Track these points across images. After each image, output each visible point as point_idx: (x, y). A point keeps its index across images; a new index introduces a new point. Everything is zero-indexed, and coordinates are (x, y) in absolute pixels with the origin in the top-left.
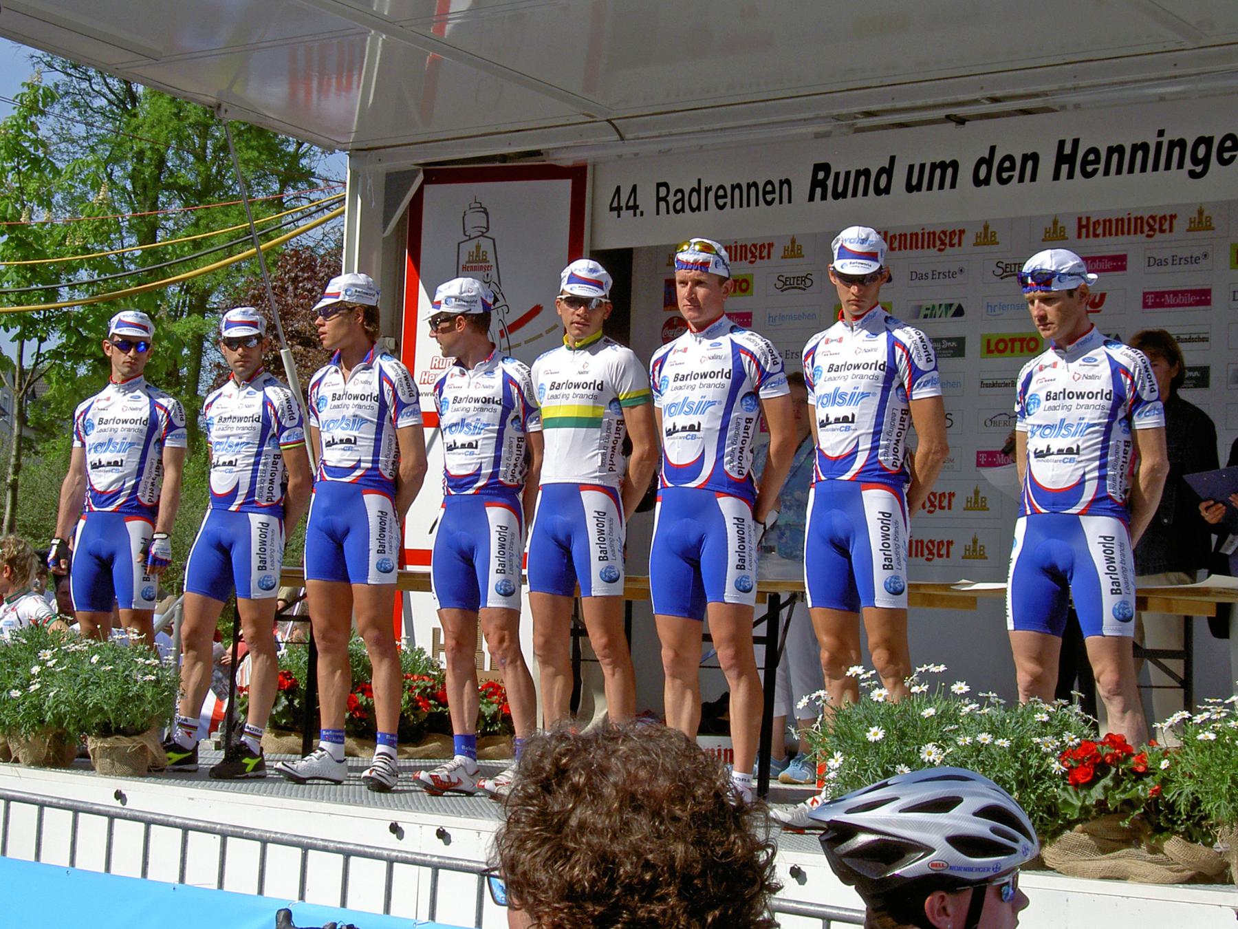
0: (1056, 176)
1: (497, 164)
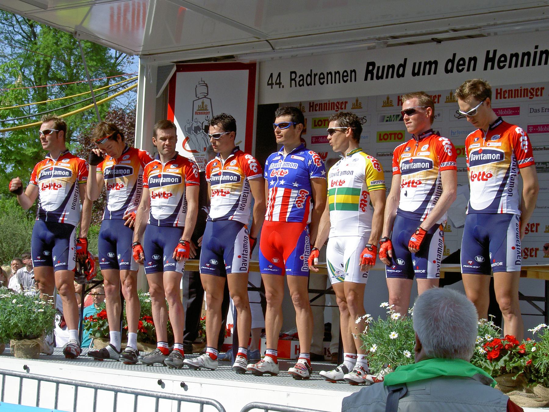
0: (485, 68)
1: (213, 62)
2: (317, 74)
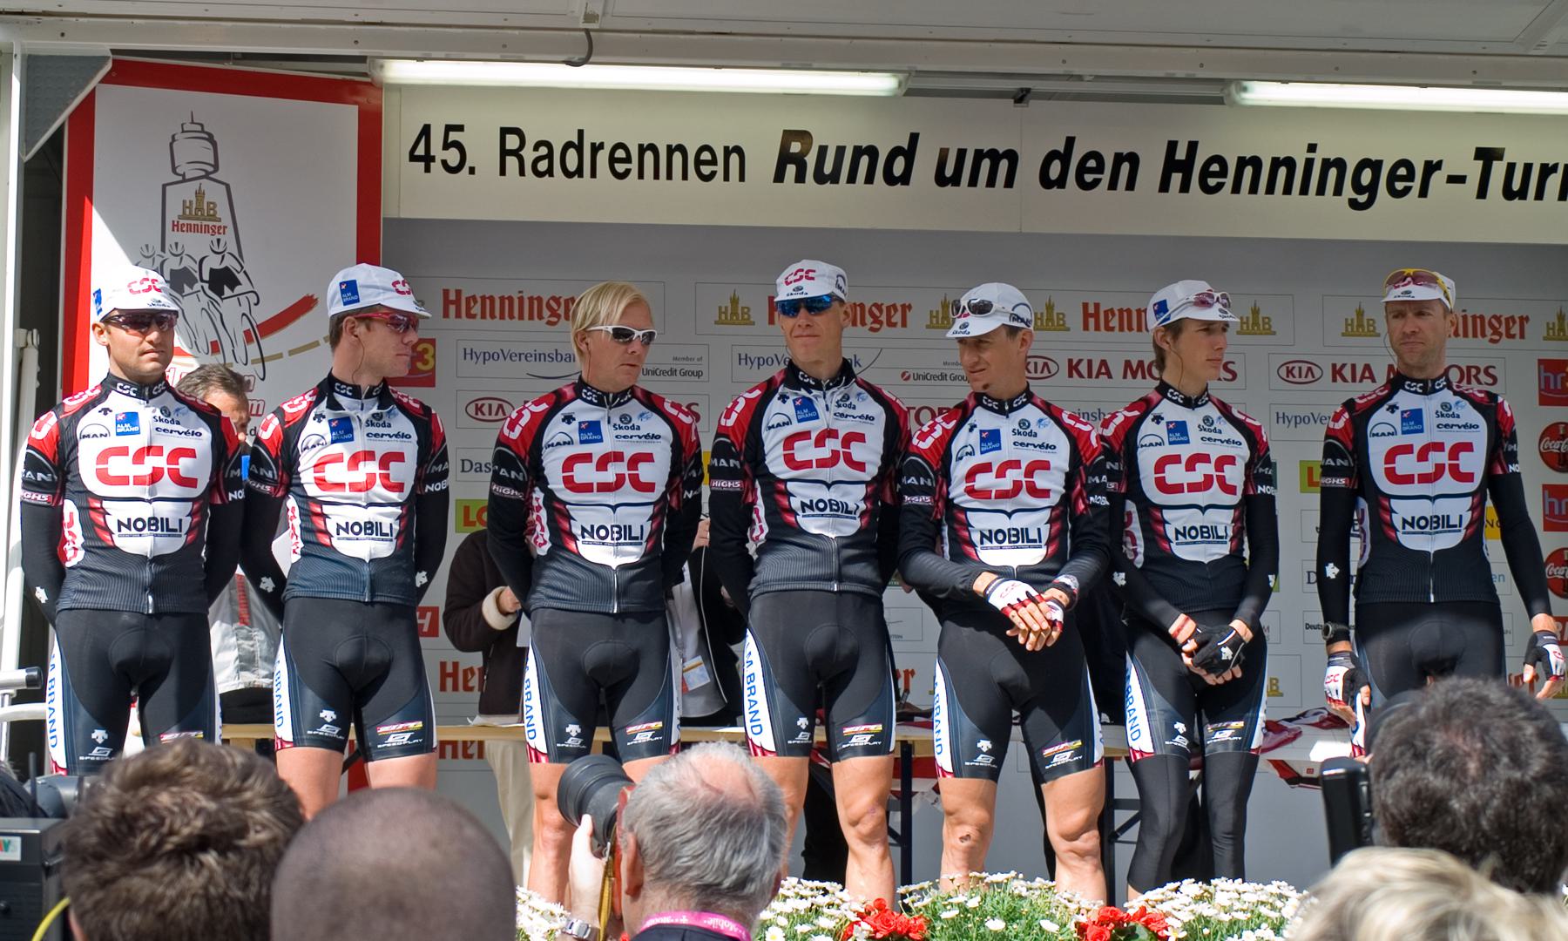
0: (1164, 187)
2: (601, 146)
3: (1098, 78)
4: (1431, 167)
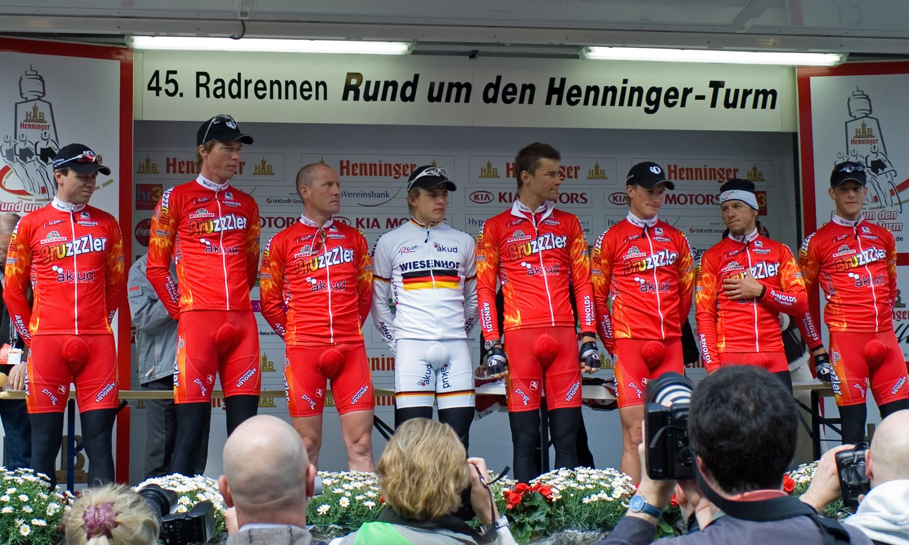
0: (548, 102)
2: (250, 81)
3: (513, 45)
4: (687, 91)
